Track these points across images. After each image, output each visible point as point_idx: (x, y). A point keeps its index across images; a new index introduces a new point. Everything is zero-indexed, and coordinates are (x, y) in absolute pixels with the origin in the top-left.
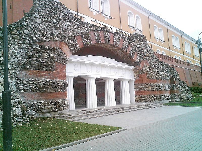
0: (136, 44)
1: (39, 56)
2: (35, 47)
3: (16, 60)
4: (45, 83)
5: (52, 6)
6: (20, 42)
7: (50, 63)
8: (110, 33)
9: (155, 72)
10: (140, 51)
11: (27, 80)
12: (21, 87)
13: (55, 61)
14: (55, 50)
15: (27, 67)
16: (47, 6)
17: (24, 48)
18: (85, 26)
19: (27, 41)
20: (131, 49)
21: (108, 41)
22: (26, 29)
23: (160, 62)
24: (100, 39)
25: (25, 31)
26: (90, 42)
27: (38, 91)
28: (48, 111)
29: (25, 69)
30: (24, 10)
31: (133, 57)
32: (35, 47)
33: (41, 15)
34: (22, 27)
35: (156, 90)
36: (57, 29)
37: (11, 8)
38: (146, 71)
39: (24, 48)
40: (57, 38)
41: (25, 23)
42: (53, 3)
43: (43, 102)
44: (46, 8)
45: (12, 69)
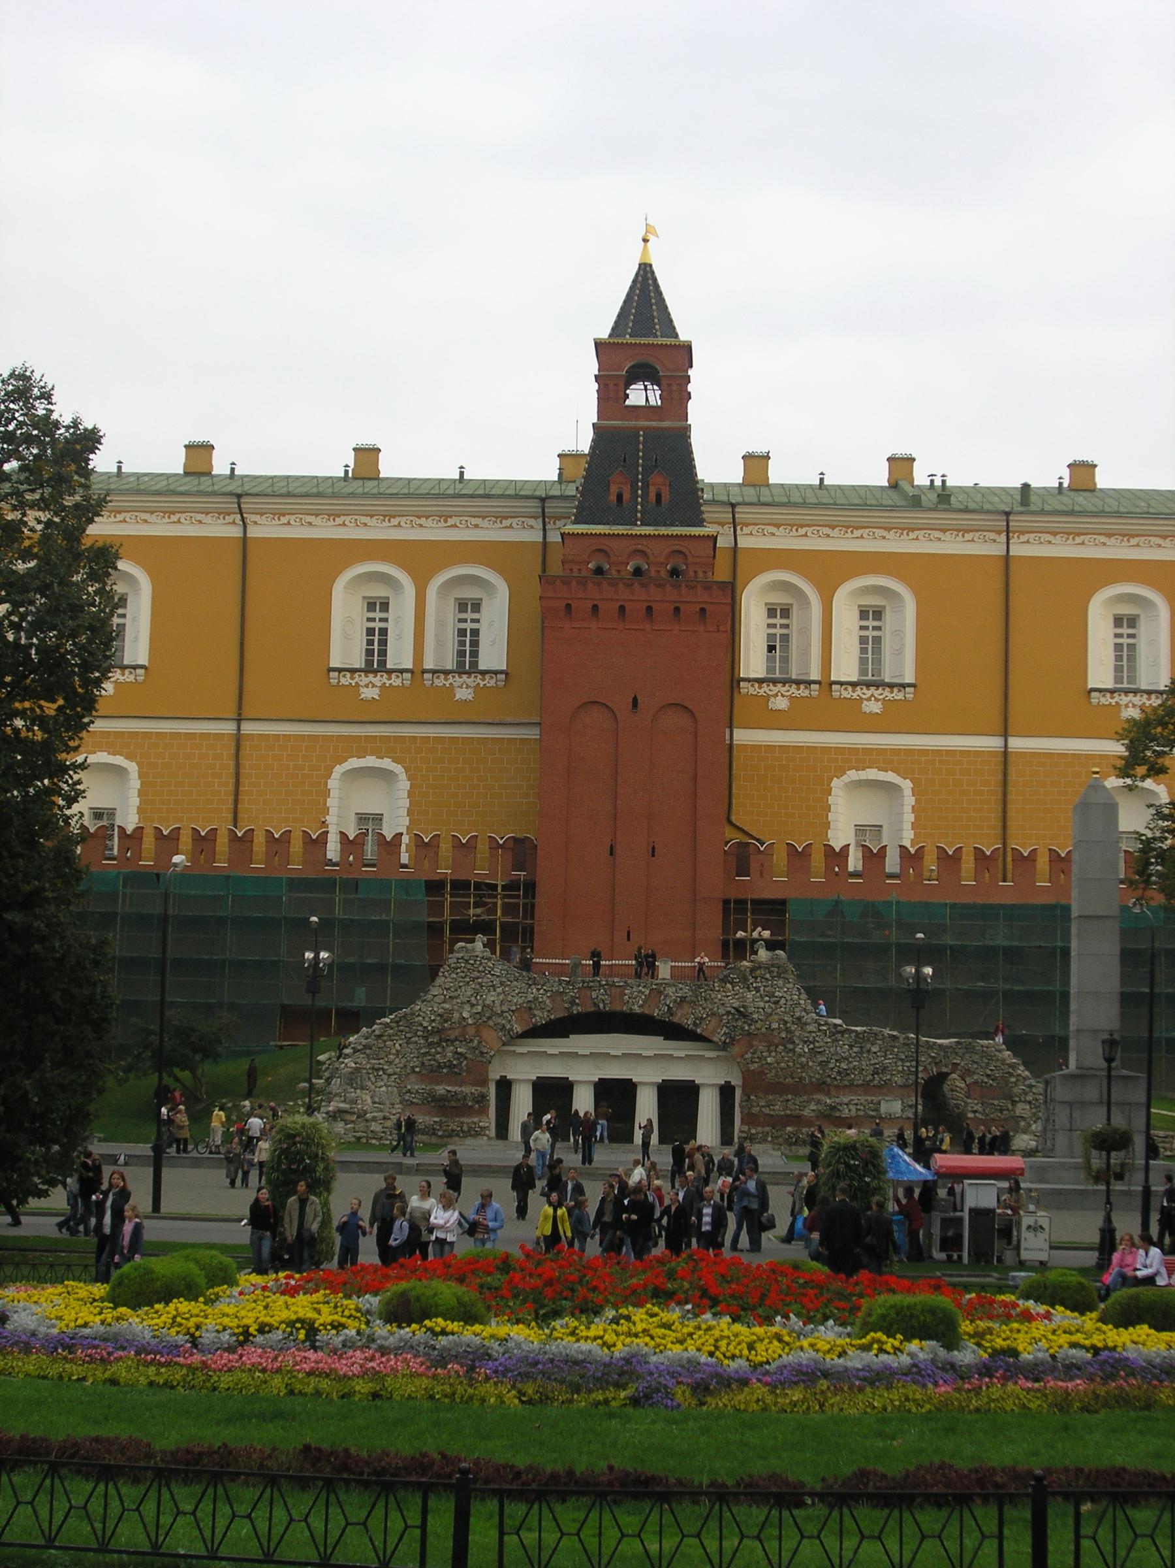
4: (443, 1092)
5: (469, 966)
13: (466, 1058)
19: (419, 1033)
21: (601, 1006)
30: (653, 848)
33: (447, 989)
36: (473, 1005)
37: (611, 854)
40: (470, 1021)
43: (437, 1119)
45: (395, 1074)
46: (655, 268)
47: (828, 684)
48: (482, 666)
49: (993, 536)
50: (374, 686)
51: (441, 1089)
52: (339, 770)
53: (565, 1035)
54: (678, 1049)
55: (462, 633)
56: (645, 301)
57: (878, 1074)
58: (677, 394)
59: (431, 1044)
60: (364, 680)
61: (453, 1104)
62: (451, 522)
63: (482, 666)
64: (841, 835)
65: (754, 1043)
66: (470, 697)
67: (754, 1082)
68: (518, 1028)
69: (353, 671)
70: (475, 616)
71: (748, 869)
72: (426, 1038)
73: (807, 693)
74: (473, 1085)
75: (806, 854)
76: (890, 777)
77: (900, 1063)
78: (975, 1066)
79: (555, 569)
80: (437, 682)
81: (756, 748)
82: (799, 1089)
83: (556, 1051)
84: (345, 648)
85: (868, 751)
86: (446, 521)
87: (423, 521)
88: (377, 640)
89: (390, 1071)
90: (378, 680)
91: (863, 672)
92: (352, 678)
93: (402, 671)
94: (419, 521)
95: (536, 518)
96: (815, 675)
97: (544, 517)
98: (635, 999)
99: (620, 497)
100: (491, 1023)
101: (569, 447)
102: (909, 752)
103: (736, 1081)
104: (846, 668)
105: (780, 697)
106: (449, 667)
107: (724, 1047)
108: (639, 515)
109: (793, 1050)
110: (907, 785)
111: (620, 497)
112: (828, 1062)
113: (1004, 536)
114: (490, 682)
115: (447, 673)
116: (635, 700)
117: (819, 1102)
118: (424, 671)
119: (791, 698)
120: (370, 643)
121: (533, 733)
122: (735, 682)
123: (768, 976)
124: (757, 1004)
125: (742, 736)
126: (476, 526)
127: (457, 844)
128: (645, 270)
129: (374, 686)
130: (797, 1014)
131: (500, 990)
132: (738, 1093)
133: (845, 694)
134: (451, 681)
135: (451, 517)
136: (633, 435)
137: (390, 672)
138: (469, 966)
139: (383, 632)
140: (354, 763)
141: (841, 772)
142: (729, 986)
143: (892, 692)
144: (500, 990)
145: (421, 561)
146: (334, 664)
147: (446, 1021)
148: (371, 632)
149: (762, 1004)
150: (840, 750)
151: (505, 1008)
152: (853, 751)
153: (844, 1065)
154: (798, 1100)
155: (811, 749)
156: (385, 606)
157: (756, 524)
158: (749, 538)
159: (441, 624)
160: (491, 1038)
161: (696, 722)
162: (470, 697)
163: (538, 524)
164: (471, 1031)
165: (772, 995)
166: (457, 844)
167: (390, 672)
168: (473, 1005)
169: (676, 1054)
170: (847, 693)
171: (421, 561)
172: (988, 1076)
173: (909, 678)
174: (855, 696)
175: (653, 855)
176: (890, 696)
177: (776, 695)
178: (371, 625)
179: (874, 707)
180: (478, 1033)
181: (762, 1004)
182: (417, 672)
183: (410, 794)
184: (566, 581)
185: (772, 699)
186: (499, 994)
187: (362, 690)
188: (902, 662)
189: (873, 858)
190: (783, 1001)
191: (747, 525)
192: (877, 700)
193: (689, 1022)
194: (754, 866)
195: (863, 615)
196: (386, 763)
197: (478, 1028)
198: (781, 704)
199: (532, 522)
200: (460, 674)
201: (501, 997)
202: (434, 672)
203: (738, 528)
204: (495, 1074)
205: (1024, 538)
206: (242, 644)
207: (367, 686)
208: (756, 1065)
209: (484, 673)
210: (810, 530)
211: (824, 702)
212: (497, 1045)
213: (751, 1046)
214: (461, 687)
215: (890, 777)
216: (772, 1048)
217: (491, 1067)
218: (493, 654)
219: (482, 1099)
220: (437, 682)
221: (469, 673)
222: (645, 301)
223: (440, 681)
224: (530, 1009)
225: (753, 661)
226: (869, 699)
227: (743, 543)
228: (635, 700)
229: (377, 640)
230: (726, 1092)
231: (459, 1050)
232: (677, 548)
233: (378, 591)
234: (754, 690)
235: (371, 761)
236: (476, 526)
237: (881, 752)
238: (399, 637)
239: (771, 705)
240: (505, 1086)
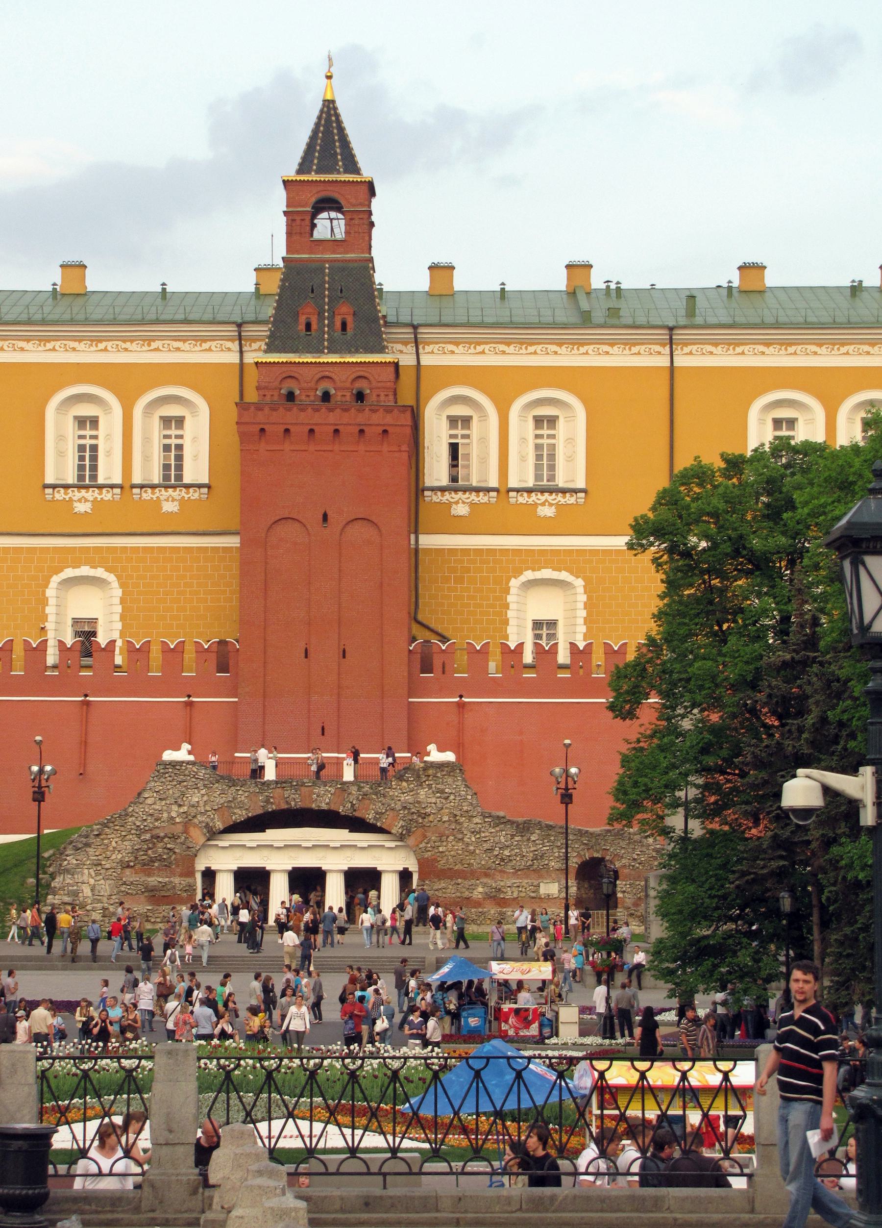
0: (396, 794)
1: (150, 849)
2: (142, 838)
3: (120, 856)
5: (176, 772)
6: (123, 833)
7: (165, 857)
8: (303, 788)
9: (477, 852)
10: (405, 808)
11: (131, 880)
12: (123, 889)
13: (175, 853)
14: (174, 837)
15: (132, 864)
17: (130, 840)
18: (238, 788)
19: (133, 832)
21: (293, 803)
22: (131, 816)
23: (512, 823)
25: (130, 820)
27: (146, 894)
28: (158, 920)
29: (128, 866)
30: (344, 651)
31: (379, 824)
32: (142, 838)
34: (127, 815)
35: (480, 896)
37: (306, 657)
39: (130, 840)
40: (178, 820)
41: (131, 809)
43: (150, 908)
46: (338, 104)
47: (503, 491)
48: (187, 480)
49: (658, 348)
50: (86, 501)
51: (153, 880)
52: (55, 580)
54: (362, 839)
56: (329, 141)
57: (536, 859)
58: (362, 225)
59: (145, 841)
60: (77, 494)
61: (163, 893)
62: (154, 345)
63: (187, 480)
64: (519, 634)
65: (428, 834)
66: (176, 509)
67: (428, 868)
68: (220, 825)
69: (66, 487)
70: (179, 432)
71: (431, 665)
72: (139, 836)
73: (486, 499)
74: (181, 875)
75: (484, 651)
76: (564, 575)
77: (556, 850)
78: (623, 851)
79: (252, 396)
80: (144, 496)
81: (440, 552)
82: (470, 874)
83: (254, 844)
84: (60, 465)
85: (543, 552)
86: (149, 345)
87: (128, 345)
88: (88, 457)
89: (108, 866)
90: (91, 494)
91: (538, 477)
92: (66, 494)
93: (112, 486)
94: (124, 346)
95: (232, 341)
96: (493, 483)
97: (240, 340)
98: (323, 798)
99: (308, 327)
100: (196, 820)
101: (265, 261)
102: (581, 552)
103: (413, 867)
104: (522, 474)
106: (156, 481)
107: (401, 838)
108: (326, 343)
109: (462, 839)
110: (579, 583)
111: (308, 327)
112: (491, 850)
113: (668, 348)
114: (194, 494)
115: (153, 487)
116: (325, 517)
117: (485, 885)
118: (133, 486)
119: (472, 505)
120: (82, 458)
121: (234, 541)
122: (419, 490)
123: (439, 775)
124: (429, 800)
125: (426, 541)
126: (178, 349)
127: (166, 650)
128: (328, 107)
129: (86, 501)
130: (465, 808)
131: (203, 792)
132: (415, 877)
133: (521, 500)
135: (154, 341)
136: (317, 269)
137: (100, 487)
138: (176, 772)
139: (94, 448)
140: (69, 573)
141: (518, 573)
142: (404, 784)
143: (564, 497)
144: (203, 792)
145: (127, 383)
146: (49, 479)
147: (157, 820)
148: (82, 448)
149: (433, 800)
150: (517, 552)
151: (208, 808)
152: (530, 552)
153: (507, 853)
154: (467, 883)
155: (491, 552)
156: (94, 422)
157: (437, 343)
158: (430, 356)
159: (147, 440)
160: (198, 836)
161: (381, 536)
163: (235, 346)
164: (179, 829)
165: (442, 792)
166: (166, 650)
167: (100, 487)
168: (180, 806)
169: (360, 844)
170: (523, 499)
171: (127, 383)
172: (634, 859)
173: (581, 484)
174: (530, 501)
175: (344, 657)
176: (563, 501)
177: (457, 503)
178: (82, 442)
179: (547, 512)
180: (186, 831)
182: (126, 487)
183: (123, 601)
184: (259, 407)
185: (454, 506)
186: (203, 795)
187: (75, 504)
188: (572, 470)
189: (545, 654)
190: (452, 797)
191: (429, 344)
192: (551, 505)
193: (370, 817)
194: (437, 663)
195: (539, 421)
196: (100, 572)
197: (187, 825)
198: (461, 510)
199: (229, 344)
200: (167, 487)
201: (205, 798)
202: (142, 487)
203: (420, 347)
204: (201, 865)
205: (686, 350)
207: (79, 501)
208: (429, 853)
209: (188, 486)
210: (487, 347)
211: (502, 506)
212: (202, 840)
213: (425, 837)
214: (167, 500)
215: (564, 575)
216: (444, 838)
217: (197, 860)
218: (196, 469)
219: (191, 889)
220: (144, 496)
221: (174, 487)
222: (329, 141)
223: (147, 495)
225: (436, 470)
226: (543, 504)
227: (425, 360)
228: (325, 517)
229: (88, 457)
230: (405, 876)
231: (169, 846)
232: (362, 374)
233: (86, 410)
234: (437, 497)
235: (85, 571)
236: (178, 349)
237: (555, 552)
238: (109, 453)
239: (453, 512)
240: (210, 875)
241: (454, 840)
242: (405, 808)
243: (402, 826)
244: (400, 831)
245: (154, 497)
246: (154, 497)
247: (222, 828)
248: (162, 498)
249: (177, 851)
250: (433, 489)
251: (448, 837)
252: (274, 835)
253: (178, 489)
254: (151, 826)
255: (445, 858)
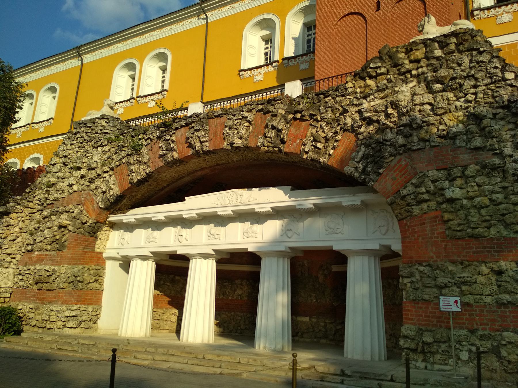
15: (29, 248)
16: (78, 136)
20: (314, 131)
24: (172, 150)
26: (144, 170)
38: (440, 199)
42: (88, 125)
44: (77, 138)
50: (260, 73)
53: (182, 199)
55: (309, 41)
80: (290, 63)
100: (93, 186)
105: (505, 14)
116: (379, 3)
123: (438, 53)
129: (260, 73)
134: (297, 61)
142: (370, 82)
144: (106, 149)
146: (242, 68)
151: (106, 168)
162: (307, 67)
181: (428, 98)
206: (204, 69)
224: (129, 164)
228: (379, 3)
241: (479, 173)
242: (370, 122)
243: (364, 157)
244: (361, 166)
245: (296, 63)
246: (296, 63)
247: (116, 190)
248: (300, 63)
249: (70, 228)
250: (481, 9)
251: (465, 167)
252: (194, 204)
253: (309, 55)
254: (52, 198)
255: (462, 213)
